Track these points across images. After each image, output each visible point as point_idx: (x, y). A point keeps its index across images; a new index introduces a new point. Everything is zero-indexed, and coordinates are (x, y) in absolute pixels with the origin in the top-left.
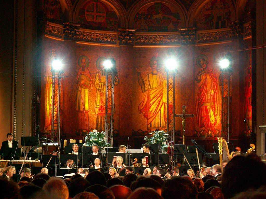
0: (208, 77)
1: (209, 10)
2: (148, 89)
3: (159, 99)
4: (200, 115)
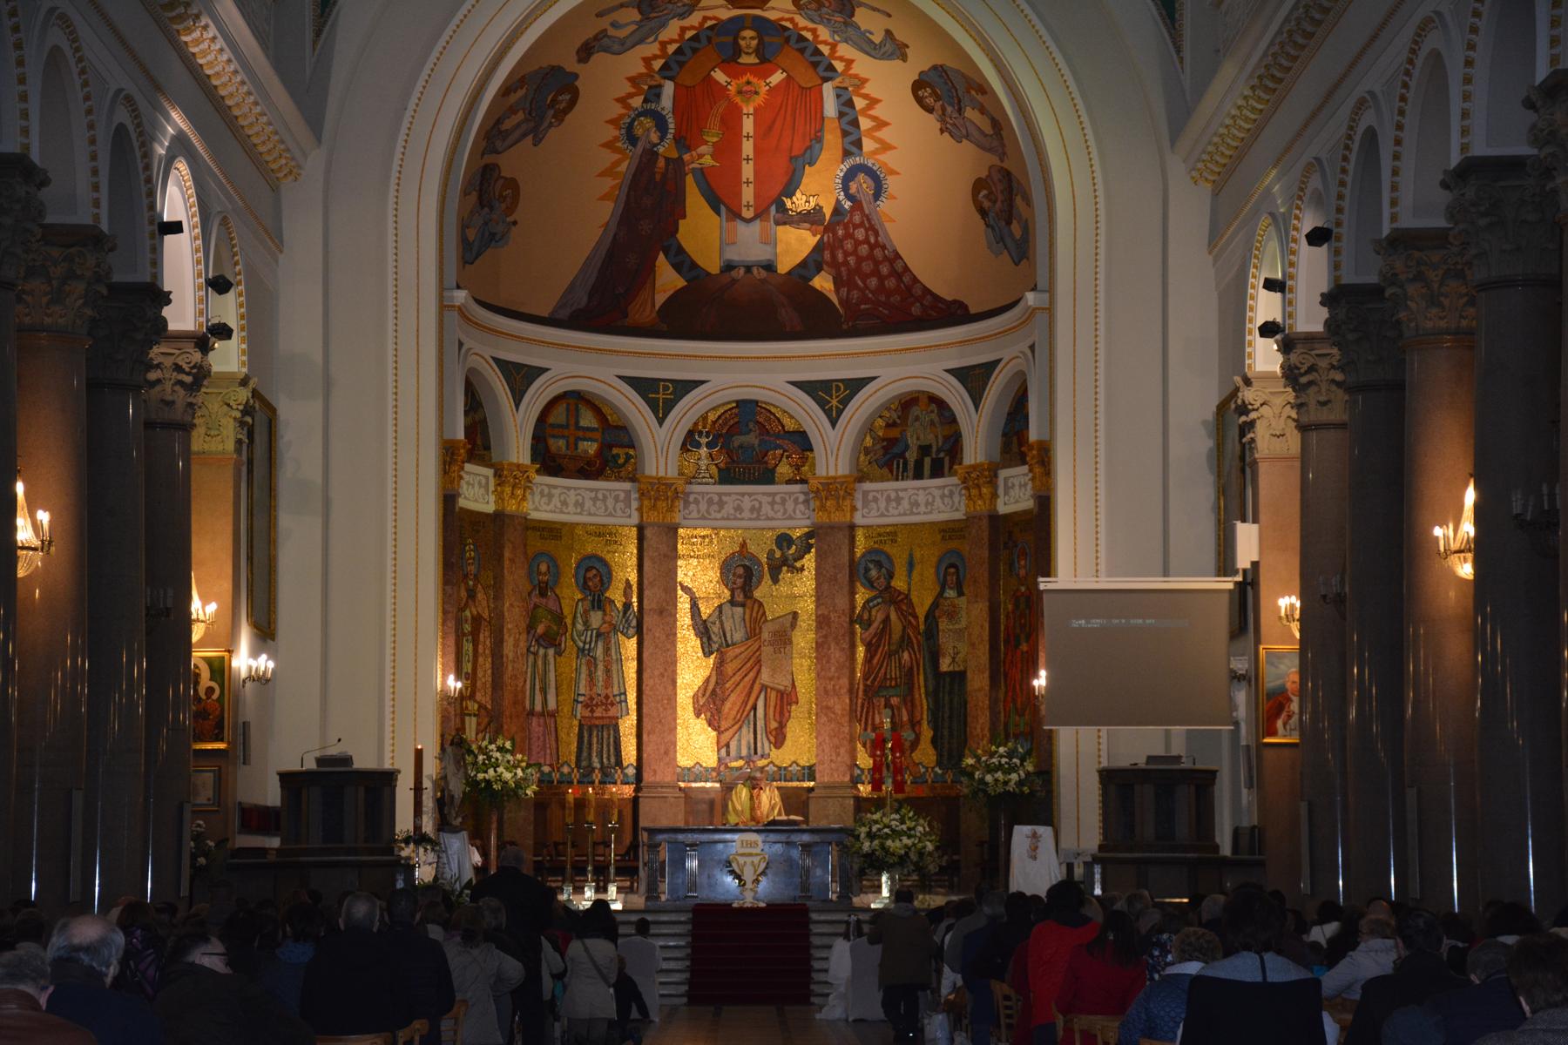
0: (893, 616)
1: (894, 424)
2: (721, 646)
3: (752, 675)
4: (870, 722)
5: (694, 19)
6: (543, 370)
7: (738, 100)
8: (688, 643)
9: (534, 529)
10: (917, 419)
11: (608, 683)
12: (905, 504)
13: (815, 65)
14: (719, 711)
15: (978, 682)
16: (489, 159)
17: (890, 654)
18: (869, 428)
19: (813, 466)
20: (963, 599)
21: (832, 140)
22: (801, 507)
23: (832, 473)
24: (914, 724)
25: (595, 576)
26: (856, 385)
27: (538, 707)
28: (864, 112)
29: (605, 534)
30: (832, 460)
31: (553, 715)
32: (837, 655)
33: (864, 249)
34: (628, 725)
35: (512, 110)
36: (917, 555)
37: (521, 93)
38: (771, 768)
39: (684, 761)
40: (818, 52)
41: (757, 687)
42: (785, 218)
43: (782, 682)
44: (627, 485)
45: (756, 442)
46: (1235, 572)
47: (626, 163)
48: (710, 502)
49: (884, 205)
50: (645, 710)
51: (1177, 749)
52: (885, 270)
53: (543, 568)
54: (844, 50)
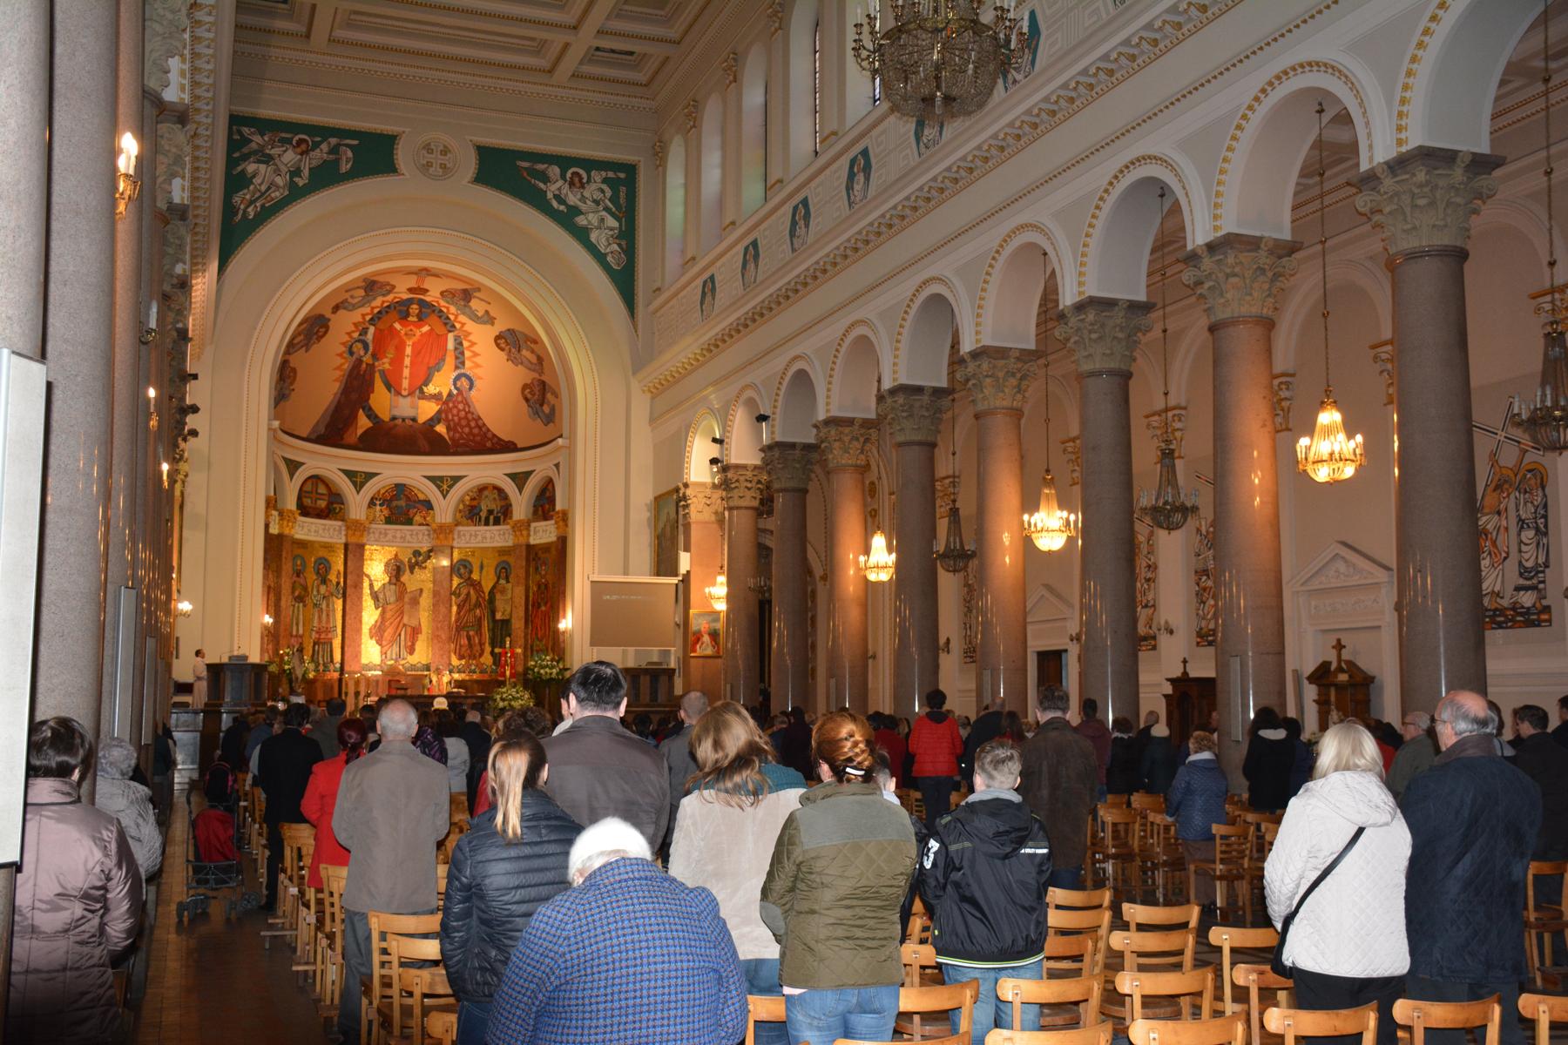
0: (472, 592)
5: (390, 297)
6: (303, 464)
7: (405, 338)
8: (368, 603)
9: (298, 543)
10: (486, 497)
11: (328, 621)
12: (479, 538)
13: (446, 324)
14: (382, 637)
15: (518, 624)
16: (287, 357)
17: (470, 610)
18: (462, 500)
19: (434, 517)
20: (509, 586)
21: (450, 360)
22: (426, 537)
23: (443, 521)
24: (481, 644)
25: (323, 568)
26: (456, 479)
27: (294, 633)
28: (468, 348)
29: (329, 547)
30: (443, 515)
31: (301, 637)
32: (443, 610)
33: (462, 414)
34: (337, 643)
35: (299, 334)
36: (485, 562)
37: (305, 325)
38: (407, 665)
39: (364, 661)
40: (448, 318)
41: (401, 625)
42: (423, 396)
43: (414, 623)
44: (340, 523)
45: (404, 504)
46: (676, 575)
47: (346, 365)
48: (380, 533)
49: (473, 393)
50: (346, 635)
51: (655, 659)
52: (473, 424)
53: (299, 562)
54: (462, 318)
